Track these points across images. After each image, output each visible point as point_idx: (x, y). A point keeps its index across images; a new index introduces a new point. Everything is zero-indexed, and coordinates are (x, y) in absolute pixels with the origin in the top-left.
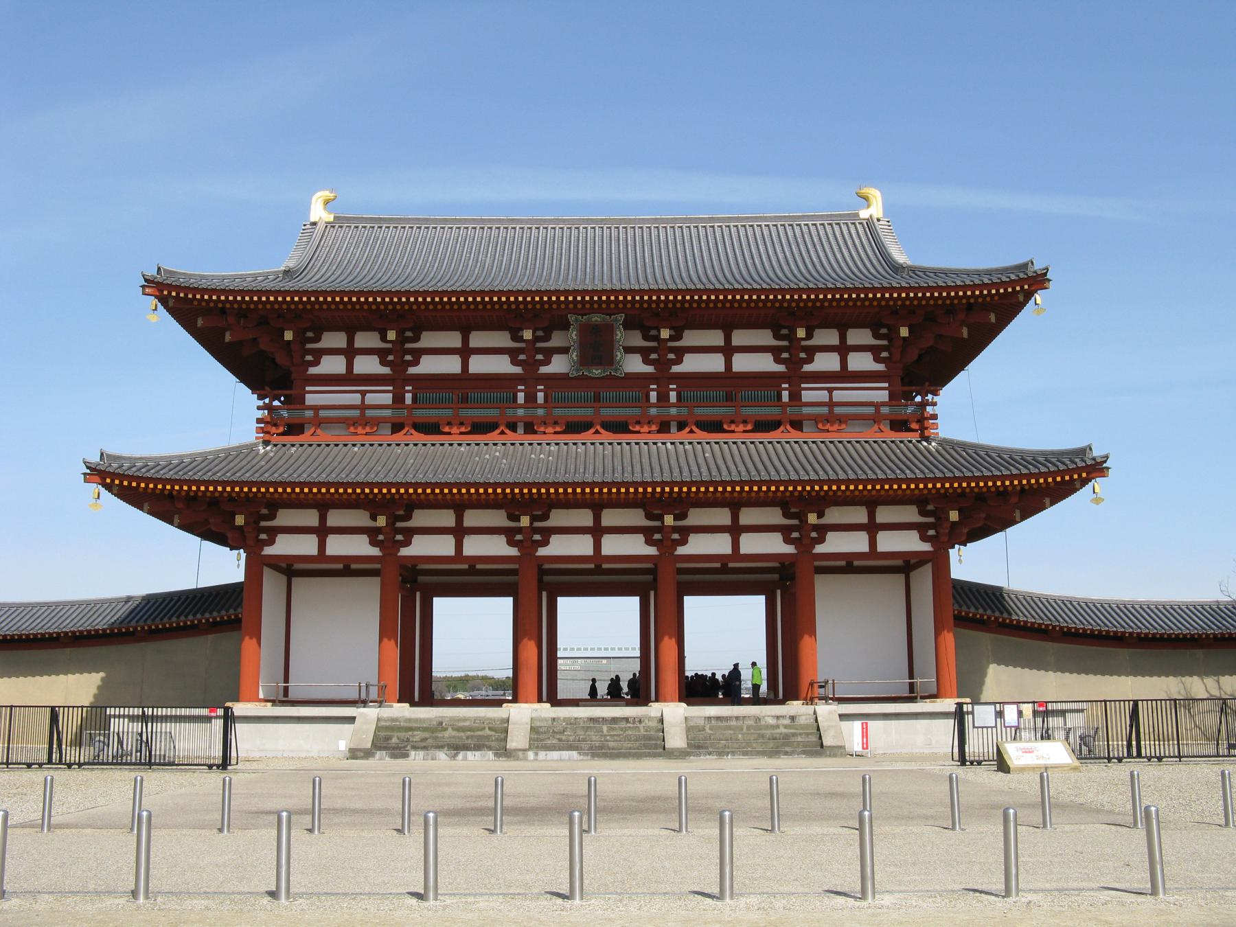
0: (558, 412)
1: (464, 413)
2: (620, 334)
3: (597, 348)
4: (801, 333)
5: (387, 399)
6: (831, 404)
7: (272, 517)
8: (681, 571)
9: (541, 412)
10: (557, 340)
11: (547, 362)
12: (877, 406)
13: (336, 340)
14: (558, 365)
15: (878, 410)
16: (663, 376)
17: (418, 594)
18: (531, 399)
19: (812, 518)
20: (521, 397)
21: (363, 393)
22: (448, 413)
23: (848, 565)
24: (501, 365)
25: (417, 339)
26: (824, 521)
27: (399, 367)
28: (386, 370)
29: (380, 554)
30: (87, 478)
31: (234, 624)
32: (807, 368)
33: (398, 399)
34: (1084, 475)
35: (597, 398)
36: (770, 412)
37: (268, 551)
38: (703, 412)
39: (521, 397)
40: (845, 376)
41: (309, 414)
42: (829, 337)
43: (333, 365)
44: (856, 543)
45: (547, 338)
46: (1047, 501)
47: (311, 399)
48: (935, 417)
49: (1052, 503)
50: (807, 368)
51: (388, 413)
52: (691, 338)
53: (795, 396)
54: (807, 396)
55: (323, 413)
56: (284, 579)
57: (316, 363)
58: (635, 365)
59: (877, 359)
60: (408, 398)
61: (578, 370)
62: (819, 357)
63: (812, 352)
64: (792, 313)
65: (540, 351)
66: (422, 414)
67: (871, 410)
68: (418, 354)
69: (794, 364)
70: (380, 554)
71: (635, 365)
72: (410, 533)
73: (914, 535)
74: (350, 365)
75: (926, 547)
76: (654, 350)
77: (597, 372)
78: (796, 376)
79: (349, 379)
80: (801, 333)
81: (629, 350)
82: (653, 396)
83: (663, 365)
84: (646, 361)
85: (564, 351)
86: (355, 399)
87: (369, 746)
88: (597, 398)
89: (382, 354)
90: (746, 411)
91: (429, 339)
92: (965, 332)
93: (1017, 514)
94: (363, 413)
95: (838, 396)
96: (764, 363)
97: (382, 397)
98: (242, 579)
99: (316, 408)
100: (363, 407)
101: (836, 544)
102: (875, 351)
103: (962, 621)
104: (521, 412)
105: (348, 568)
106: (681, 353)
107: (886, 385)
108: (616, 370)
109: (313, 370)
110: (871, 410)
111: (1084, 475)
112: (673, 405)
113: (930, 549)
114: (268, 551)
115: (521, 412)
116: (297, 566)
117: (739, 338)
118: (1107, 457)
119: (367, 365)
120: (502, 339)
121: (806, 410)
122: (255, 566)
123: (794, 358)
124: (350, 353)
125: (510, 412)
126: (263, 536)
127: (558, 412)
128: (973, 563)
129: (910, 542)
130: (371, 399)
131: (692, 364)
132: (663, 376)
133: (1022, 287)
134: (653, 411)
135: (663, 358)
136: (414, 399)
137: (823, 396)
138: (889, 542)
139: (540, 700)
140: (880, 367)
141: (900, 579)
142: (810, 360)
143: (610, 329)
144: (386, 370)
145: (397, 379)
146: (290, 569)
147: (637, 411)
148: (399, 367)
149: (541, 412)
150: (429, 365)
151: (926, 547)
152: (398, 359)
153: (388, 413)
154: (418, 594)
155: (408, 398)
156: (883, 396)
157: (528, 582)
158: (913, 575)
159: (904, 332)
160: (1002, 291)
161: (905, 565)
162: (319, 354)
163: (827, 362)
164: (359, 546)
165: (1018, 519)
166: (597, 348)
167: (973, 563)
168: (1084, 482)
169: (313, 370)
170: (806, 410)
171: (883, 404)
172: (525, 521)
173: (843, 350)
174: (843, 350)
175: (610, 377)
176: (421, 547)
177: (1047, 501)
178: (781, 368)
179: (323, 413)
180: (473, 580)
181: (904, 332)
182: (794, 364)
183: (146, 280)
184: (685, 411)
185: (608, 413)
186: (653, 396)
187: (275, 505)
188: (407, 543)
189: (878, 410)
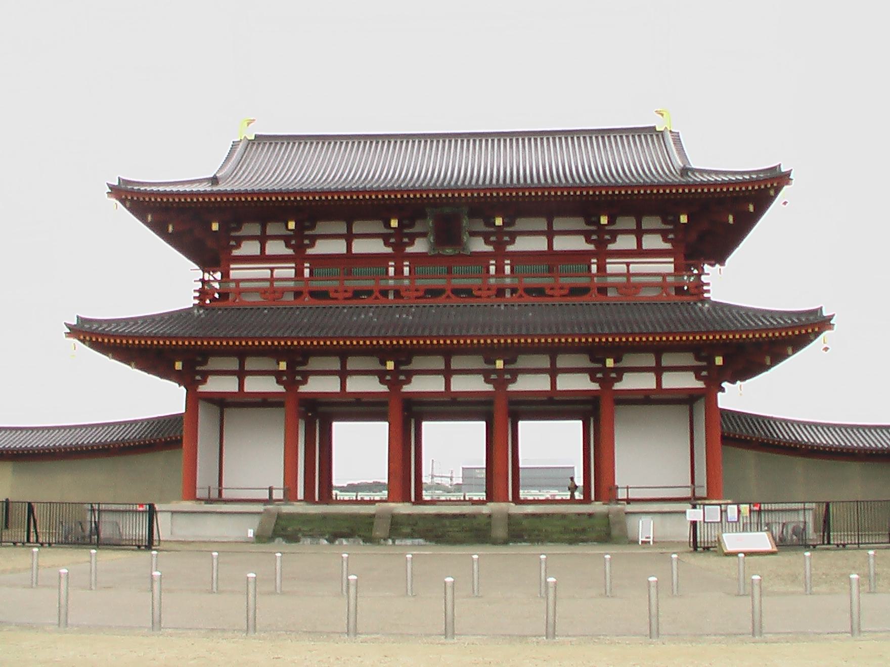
0: (419, 282)
1: (347, 283)
2: (465, 222)
3: (448, 233)
4: (604, 220)
5: (291, 273)
6: (628, 275)
7: (205, 363)
8: (512, 403)
9: (406, 282)
10: (418, 228)
11: (411, 243)
12: (664, 276)
13: (253, 229)
14: (419, 247)
15: (664, 279)
16: (500, 254)
17: (317, 421)
18: (399, 271)
19: (610, 363)
20: (391, 271)
21: (272, 269)
22: (336, 283)
23: (643, 399)
24: (376, 247)
25: (313, 227)
26: (619, 365)
27: (300, 249)
28: (290, 252)
29: (284, 390)
30: (69, 335)
31: (174, 444)
32: (611, 247)
33: (299, 272)
34: (816, 329)
35: (449, 272)
36: (583, 281)
37: (202, 388)
38: (530, 281)
39: (391, 271)
40: (640, 252)
41: (232, 285)
42: (629, 223)
44: (646, 382)
45: (412, 225)
46: (790, 351)
47: (233, 274)
48: (708, 284)
49: (794, 352)
50: (611, 247)
51: (292, 284)
52: (522, 224)
53: (602, 268)
54: (610, 268)
55: (242, 285)
56: (216, 410)
57: (238, 246)
58: (479, 246)
59: (665, 240)
60: (307, 272)
62: (620, 238)
63: (614, 235)
64: (603, 206)
65: (407, 235)
66: (317, 285)
67: (660, 279)
68: (313, 239)
69: (601, 244)
70: (284, 390)
71: (479, 246)
72: (306, 375)
73: (691, 375)
74: (263, 249)
75: (700, 385)
76: (492, 234)
77: (449, 251)
78: (602, 254)
79: (263, 258)
80: (604, 220)
81: (473, 234)
82: (492, 269)
83: (500, 246)
84: (487, 242)
85: (423, 235)
86: (266, 274)
87: (270, 533)
88: (449, 272)
89: (287, 240)
90: (563, 280)
91: (322, 228)
92: (731, 219)
93: (768, 361)
94: (272, 284)
95: (634, 268)
96: (578, 244)
97: (287, 271)
98: (184, 411)
99: (237, 281)
100: (272, 280)
101: (631, 382)
102: (664, 234)
103: (728, 440)
104: (391, 282)
105: (264, 401)
106: (513, 236)
107: (672, 260)
108: (464, 249)
109: (236, 253)
110: (660, 279)
111: (816, 329)
112: (508, 276)
113: (704, 386)
114: (202, 388)
115: (391, 282)
116: (229, 400)
117: (558, 224)
118: (833, 316)
120: (377, 227)
122: (193, 399)
123: (601, 241)
124: (263, 239)
125: (383, 283)
126: (198, 378)
127: (419, 282)
128: (735, 397)
129: (687, 381)
130: (278, 273)
131: (523, 244)
132: (500, 254)
133: (772, 185)
134: (492, 281)
135: (500, 239)
136: (311, 273)
137: (622, 268)
138: (671, 381)
139: (409, 500)
140: (668, 246)
141: (685, 409)
142: (613, 240)
144: (290, 252)
145: (299, 258)
146: (221, 402)
147: (478, 282)
148: (300, 249)
149: (406, 282)
150: (322, 248)
151: (700, 385)
152: (299, 243)
153: (292, 284)
154: (317, 421)
155: (307, 272)
156: (670, 268)
157: (395, 409)
158: (695, 405)
159: (684, 219)
160: (756, 188)
161: (687, 399)
162: (239, 241)
163: (626, 242)
164: (268, 385)
165: (768, 363)
166: (448, 233)
167: (735, 397)
168: (817, 335)
169: (236, 253)
170: (610, 280)
171: (670, 274)
172: (390, 365)
173: (639, 233)
174: (639, 233)
175: (460, 255)
176: (316, 385)
177: (790, 351)
178: (389, 250)
179: (242, 285)
180: (362, 408)
181: (684, 219)
182: (601, 244)
183: (110, 188)
184: (516, 281)
185: (457, 282)
186: (492, 269)
187: (207, 353)
188: (304, 382)
189: (664, 279)
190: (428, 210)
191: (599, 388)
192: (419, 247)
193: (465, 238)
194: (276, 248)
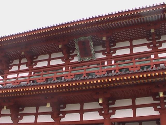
11: (73, 59)
14: (76, 60)
36: (148, 63)
43: (15, 68)
53: (156, 57)
61: (81, 59)
71: (100, 56)
77: (87, 59)
81: (96, 52)
100: (18, 78)
108: (93, 57)
119: (24, 67)
121: (160, 60)
124: (19, 65)
143: (88, 42)
150: (39, 65)
162: (12, 66)
175: (91, 61)
190: (75, 40)
191: (159, 114)
192: (76, 60)
193: (93, 52)
194: (24, 67)
